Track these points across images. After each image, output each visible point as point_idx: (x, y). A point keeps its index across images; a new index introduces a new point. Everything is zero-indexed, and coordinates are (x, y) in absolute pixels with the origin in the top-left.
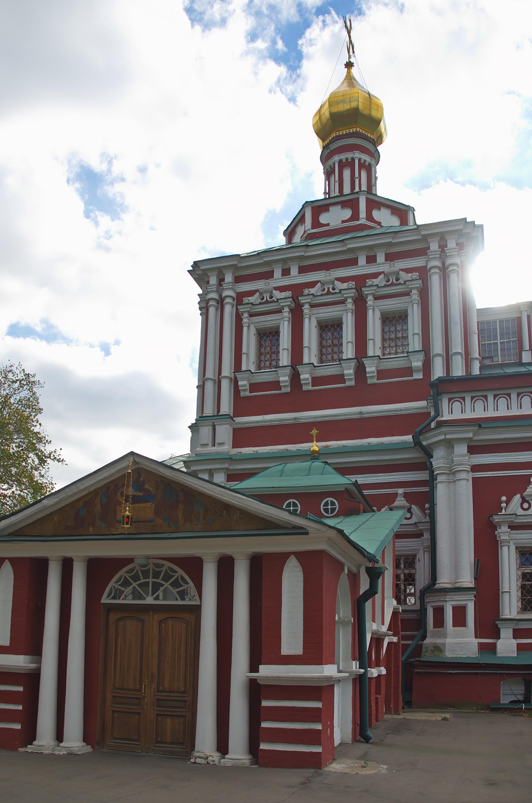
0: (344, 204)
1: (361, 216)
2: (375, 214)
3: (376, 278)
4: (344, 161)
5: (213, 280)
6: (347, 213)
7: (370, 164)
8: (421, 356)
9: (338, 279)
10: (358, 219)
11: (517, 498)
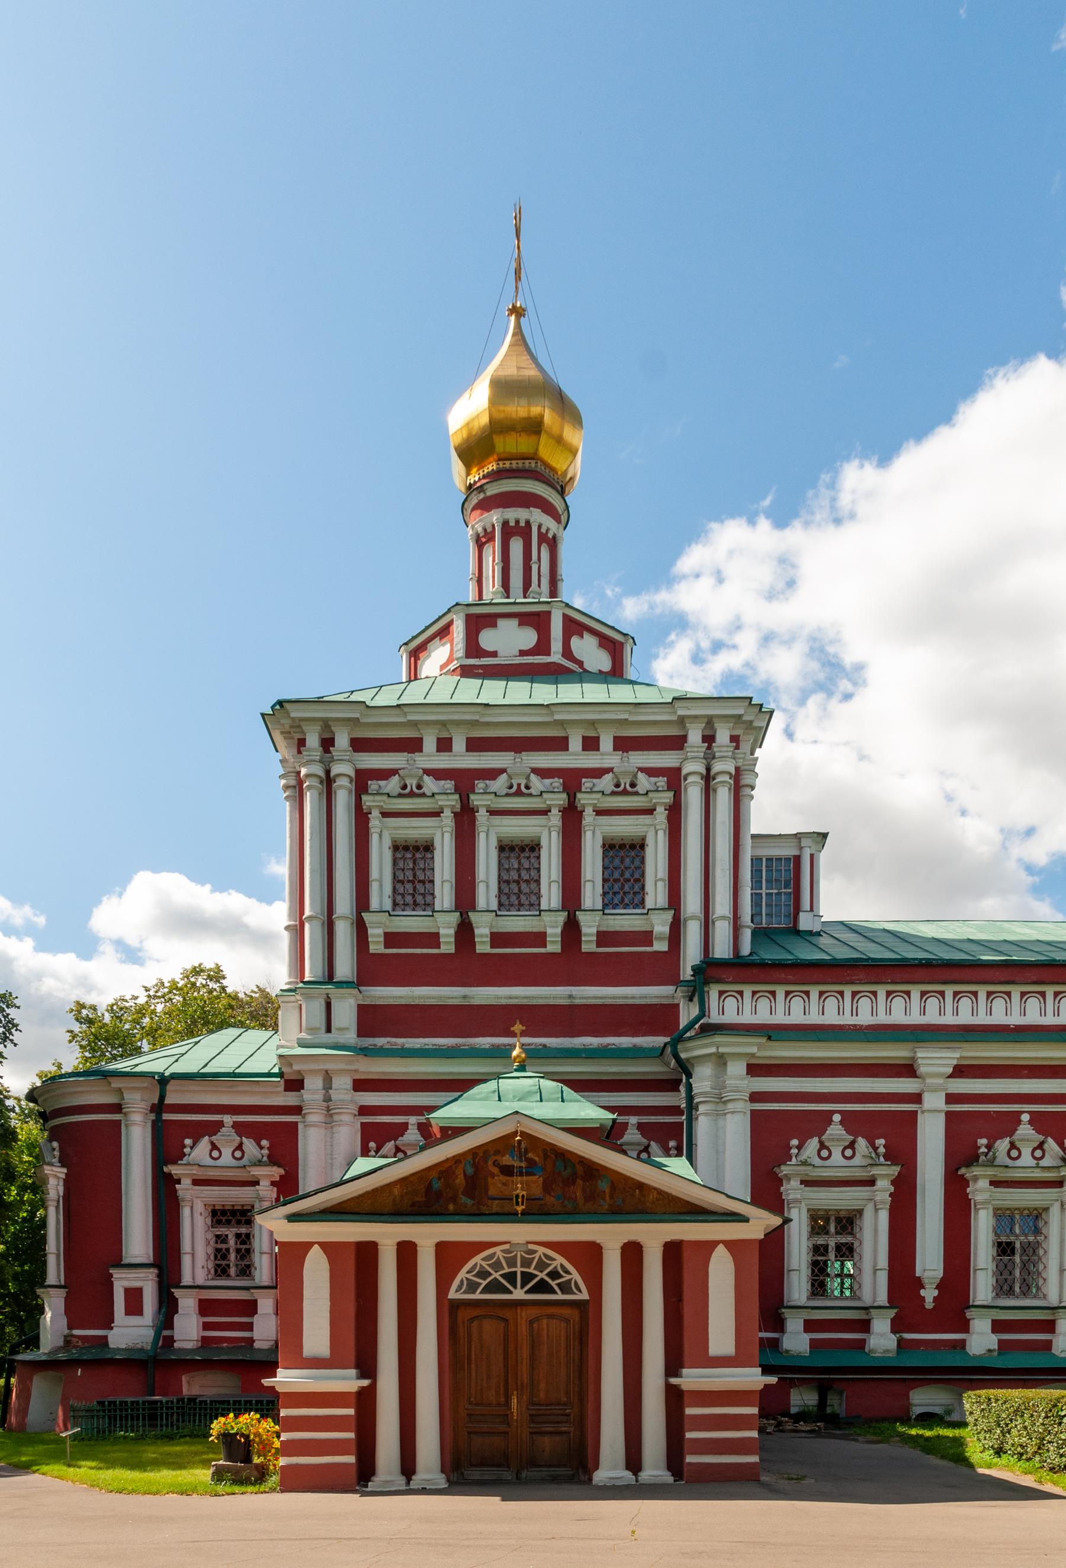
0: (526, 619)
1: (553, 649)
2: (575, 642)
3: (600, 777)
4: (512, 524)
5: (313, 741)
6: (528, 637)
7: (554, 537)
9: (536, 771)
10: (548, 654)
11: (813, 1144)
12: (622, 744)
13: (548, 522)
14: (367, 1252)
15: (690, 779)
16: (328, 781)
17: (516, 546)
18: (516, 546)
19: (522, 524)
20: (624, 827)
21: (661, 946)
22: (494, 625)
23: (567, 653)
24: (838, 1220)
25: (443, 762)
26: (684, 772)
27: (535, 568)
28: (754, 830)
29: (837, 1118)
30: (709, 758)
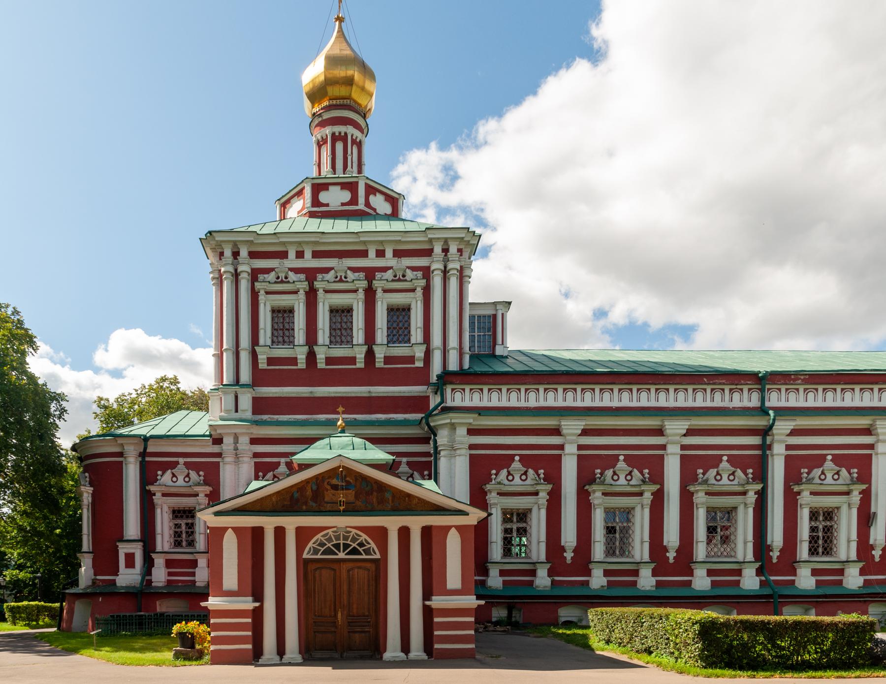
0: (344, 186)
1: (360, 202)
2: (372, 198)
4: (337, 134)
5: (228, 253)
6: (346, 196)
7: (360, 141)
8: (424, 347)
9: (350, 268)
11: (504, 472)
12: (398, 254)
13: (357, 134)
14: (258, 533)
15: (435, 273)
16: (236, 275)
17: (339, 146)
18: (339, 146)
19: (343, 134)
20: (398, 299)
21: (419, 364)
23: (367, 204)
24: (518, 515)
25: (300, 264)
26: (432, 268)
27: (349, 158)
28: (470, 301)
29: (517, 458)
30: (446, 261)
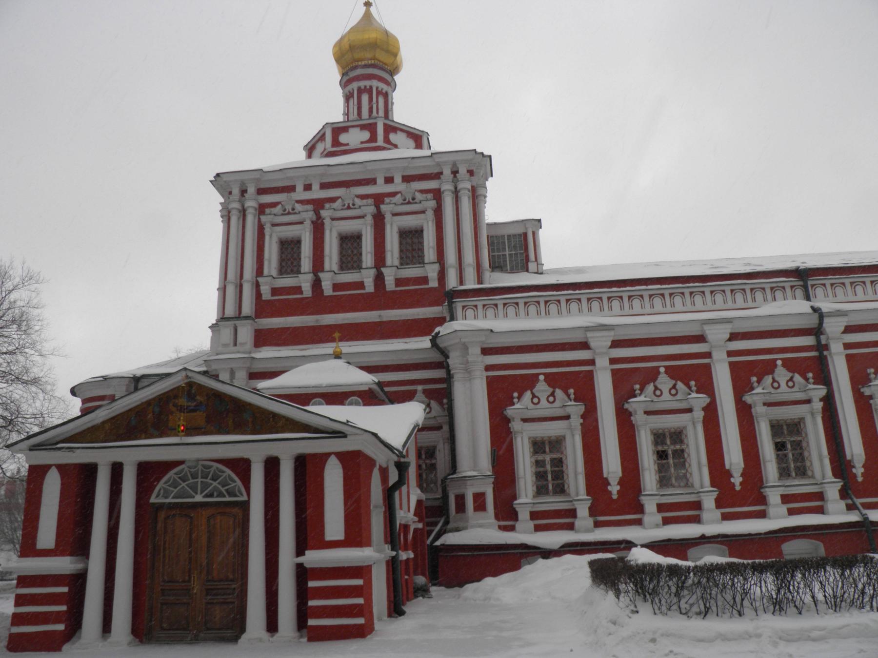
0: (363, 127)
2: (392, 137)
4: (363, 88)
6: (366, 135)
8: (437, 267)
9: (358, 196)
10: (376, 141)
11: (528, 395)
12: (407, 179)
13: (382, 86)
14: (89, 471)
15: (446, 193)
16: (243, 212)
17: (365, 98)
18: (365, 98)
20: (410, 222)
22: (347, 131)
24: (550, 442)
25: (308, 196)
